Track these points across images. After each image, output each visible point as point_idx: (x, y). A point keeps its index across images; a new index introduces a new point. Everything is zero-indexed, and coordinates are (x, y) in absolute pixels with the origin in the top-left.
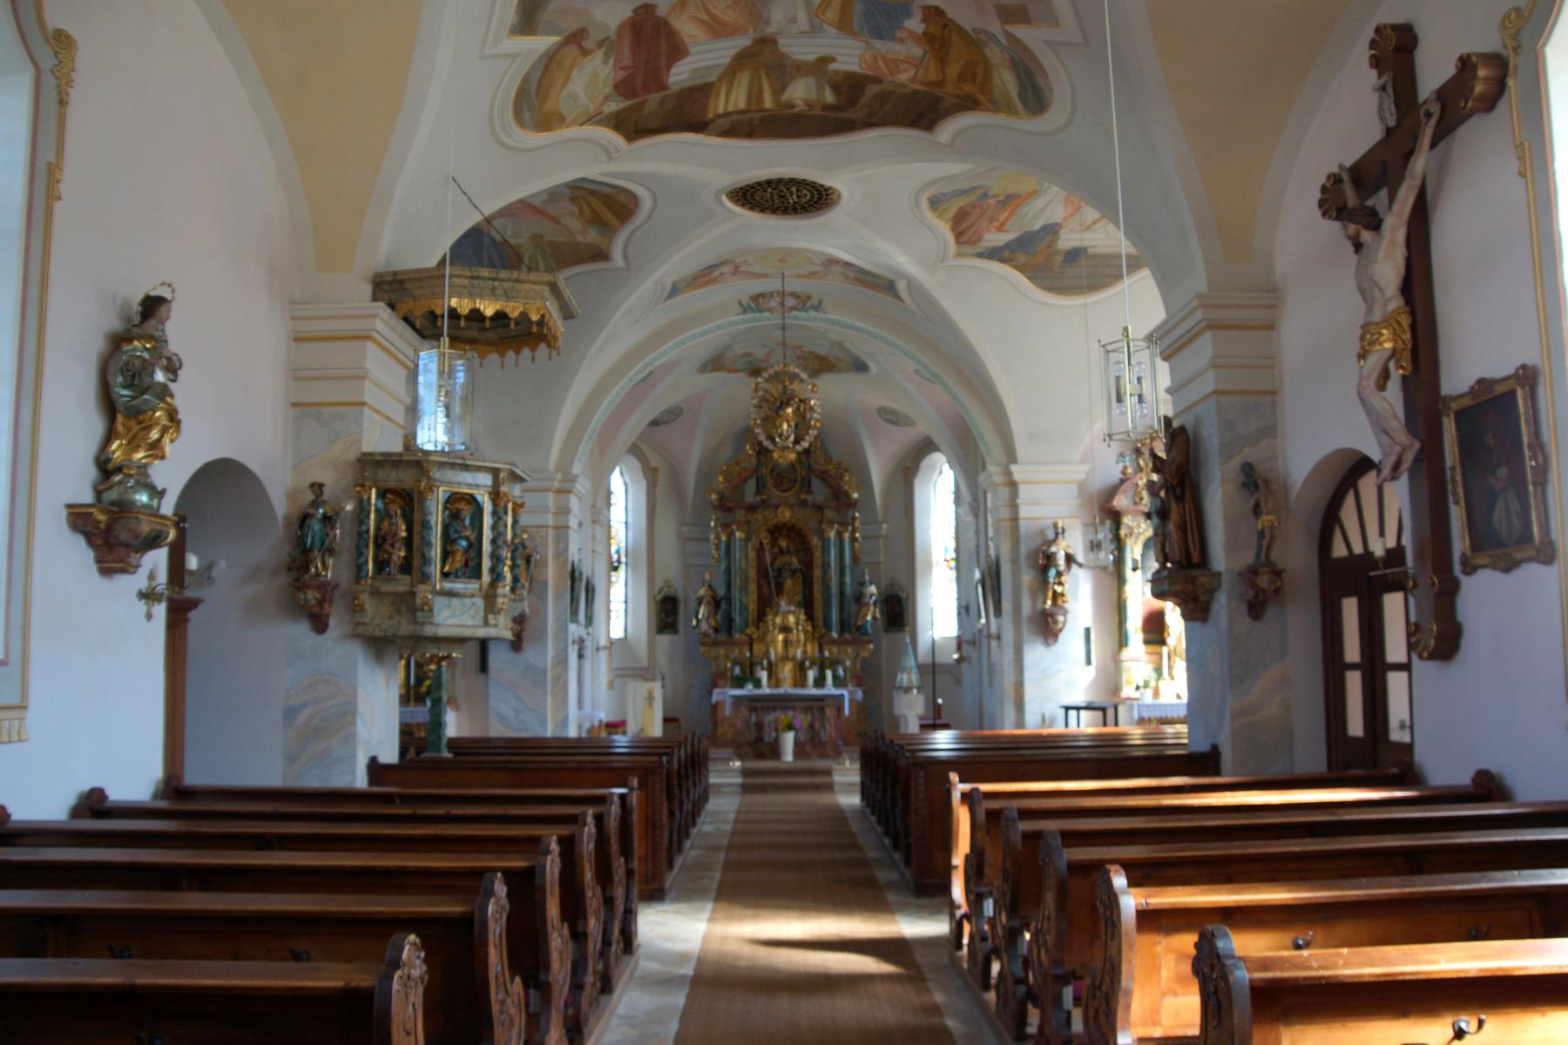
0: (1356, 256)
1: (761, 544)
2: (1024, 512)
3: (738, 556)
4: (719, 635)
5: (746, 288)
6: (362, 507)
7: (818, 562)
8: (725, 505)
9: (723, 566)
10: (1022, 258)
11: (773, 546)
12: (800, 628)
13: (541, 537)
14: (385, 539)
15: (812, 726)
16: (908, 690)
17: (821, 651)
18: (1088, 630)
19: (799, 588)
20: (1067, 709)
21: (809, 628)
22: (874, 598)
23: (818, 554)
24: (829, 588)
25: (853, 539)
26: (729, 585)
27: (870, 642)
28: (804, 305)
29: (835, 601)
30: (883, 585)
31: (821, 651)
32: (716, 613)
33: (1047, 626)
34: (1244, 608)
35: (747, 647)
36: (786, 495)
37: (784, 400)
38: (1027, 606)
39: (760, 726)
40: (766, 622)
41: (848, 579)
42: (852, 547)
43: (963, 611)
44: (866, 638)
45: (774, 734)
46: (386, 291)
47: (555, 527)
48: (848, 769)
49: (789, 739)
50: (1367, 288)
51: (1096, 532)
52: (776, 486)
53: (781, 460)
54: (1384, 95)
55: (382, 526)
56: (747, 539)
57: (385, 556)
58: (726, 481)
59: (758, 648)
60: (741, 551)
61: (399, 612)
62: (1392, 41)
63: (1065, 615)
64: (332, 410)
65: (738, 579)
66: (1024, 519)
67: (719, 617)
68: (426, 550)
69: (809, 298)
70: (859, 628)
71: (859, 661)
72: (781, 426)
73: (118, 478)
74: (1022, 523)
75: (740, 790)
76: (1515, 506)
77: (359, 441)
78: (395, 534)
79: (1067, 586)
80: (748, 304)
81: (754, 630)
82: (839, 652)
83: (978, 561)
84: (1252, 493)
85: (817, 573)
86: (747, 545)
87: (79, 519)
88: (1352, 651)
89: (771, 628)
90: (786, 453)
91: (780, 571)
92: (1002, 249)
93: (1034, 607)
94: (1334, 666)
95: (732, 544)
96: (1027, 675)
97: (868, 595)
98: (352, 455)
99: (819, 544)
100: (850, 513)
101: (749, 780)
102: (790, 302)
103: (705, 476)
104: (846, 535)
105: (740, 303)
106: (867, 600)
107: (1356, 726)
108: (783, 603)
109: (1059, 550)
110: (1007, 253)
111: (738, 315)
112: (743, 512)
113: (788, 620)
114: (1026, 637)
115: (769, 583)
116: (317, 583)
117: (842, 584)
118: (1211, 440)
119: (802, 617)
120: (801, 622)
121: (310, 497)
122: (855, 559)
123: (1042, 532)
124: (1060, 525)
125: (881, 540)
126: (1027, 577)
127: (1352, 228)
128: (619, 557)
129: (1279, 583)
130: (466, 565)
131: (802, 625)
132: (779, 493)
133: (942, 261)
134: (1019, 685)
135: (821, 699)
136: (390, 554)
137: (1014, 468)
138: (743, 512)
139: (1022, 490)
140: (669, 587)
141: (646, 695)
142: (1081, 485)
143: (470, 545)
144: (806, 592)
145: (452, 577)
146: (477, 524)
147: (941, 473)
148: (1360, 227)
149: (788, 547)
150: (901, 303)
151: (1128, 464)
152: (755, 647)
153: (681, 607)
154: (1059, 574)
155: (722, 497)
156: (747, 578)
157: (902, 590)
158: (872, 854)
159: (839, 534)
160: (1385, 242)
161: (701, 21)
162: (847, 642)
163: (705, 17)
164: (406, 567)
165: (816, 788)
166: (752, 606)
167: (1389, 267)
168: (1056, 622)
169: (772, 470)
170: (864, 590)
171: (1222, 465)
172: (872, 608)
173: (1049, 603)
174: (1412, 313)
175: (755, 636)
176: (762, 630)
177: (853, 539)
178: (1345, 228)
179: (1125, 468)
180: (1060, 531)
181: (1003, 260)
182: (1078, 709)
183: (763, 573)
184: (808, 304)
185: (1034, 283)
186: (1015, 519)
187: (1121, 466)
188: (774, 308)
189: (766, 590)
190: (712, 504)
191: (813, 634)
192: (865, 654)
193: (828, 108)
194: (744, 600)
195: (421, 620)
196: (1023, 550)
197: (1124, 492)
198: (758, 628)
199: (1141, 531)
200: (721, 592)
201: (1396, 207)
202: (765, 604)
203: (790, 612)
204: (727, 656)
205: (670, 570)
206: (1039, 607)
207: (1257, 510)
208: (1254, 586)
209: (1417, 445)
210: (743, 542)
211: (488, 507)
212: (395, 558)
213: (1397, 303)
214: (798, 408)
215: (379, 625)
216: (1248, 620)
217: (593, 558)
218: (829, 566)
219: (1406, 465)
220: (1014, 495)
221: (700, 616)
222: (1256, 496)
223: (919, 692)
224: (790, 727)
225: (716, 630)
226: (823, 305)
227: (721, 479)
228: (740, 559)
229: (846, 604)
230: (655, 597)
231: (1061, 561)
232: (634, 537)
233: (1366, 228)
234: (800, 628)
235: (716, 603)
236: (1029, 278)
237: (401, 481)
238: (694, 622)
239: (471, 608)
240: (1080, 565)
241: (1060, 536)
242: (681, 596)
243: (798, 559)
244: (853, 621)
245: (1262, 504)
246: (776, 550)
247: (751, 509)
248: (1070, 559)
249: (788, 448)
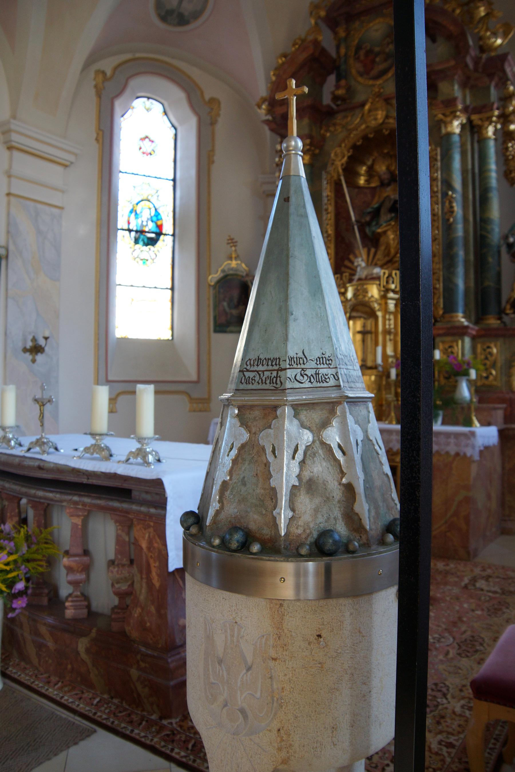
36: (379, 82)
52: (365, 73)
128: (160, 227)
132: (371, 82)
169: (358, 48)
217: (9, 204)
232: (181, 198)
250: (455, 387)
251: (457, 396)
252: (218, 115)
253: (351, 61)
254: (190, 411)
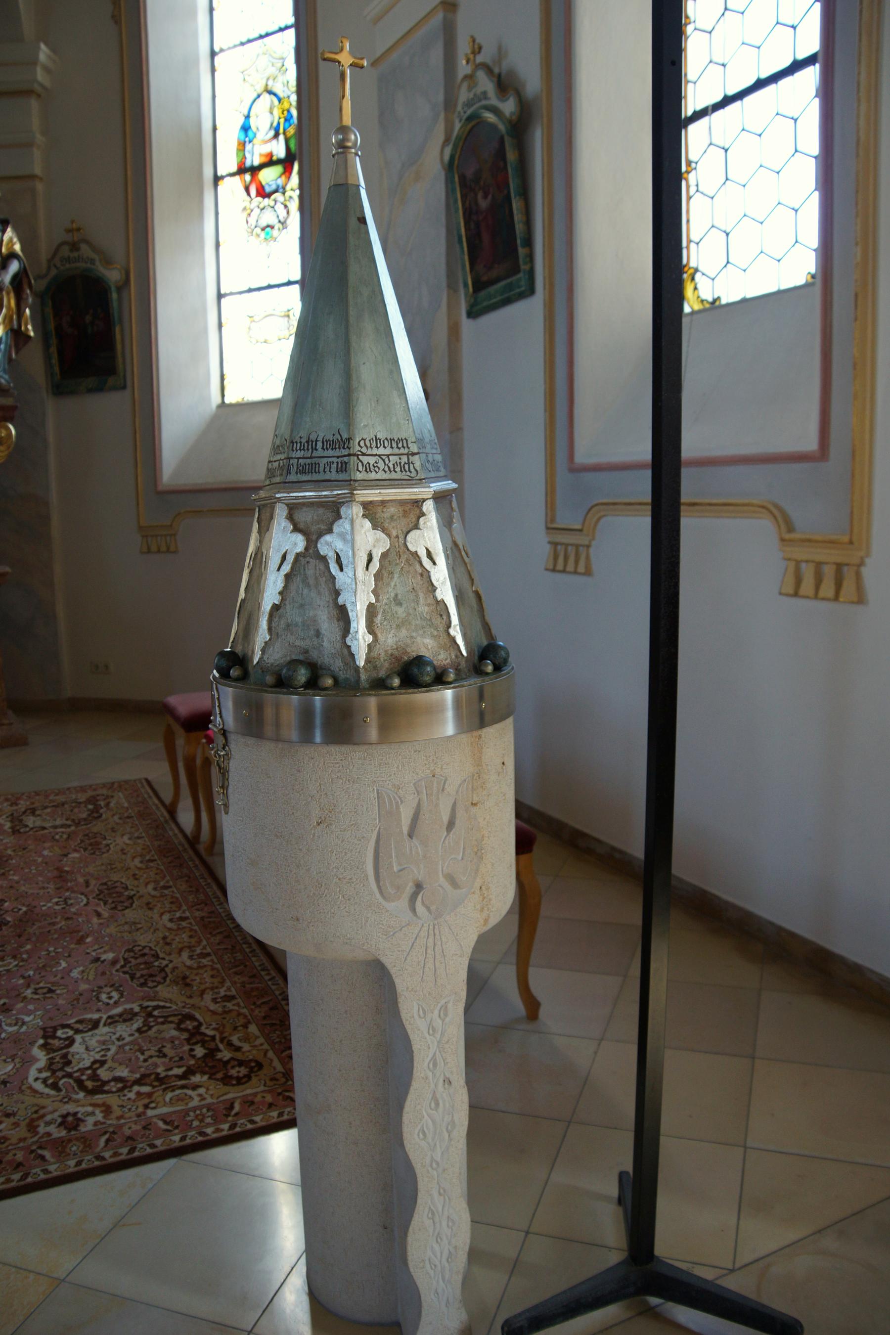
22: (14, 267)
157: (108, 262)
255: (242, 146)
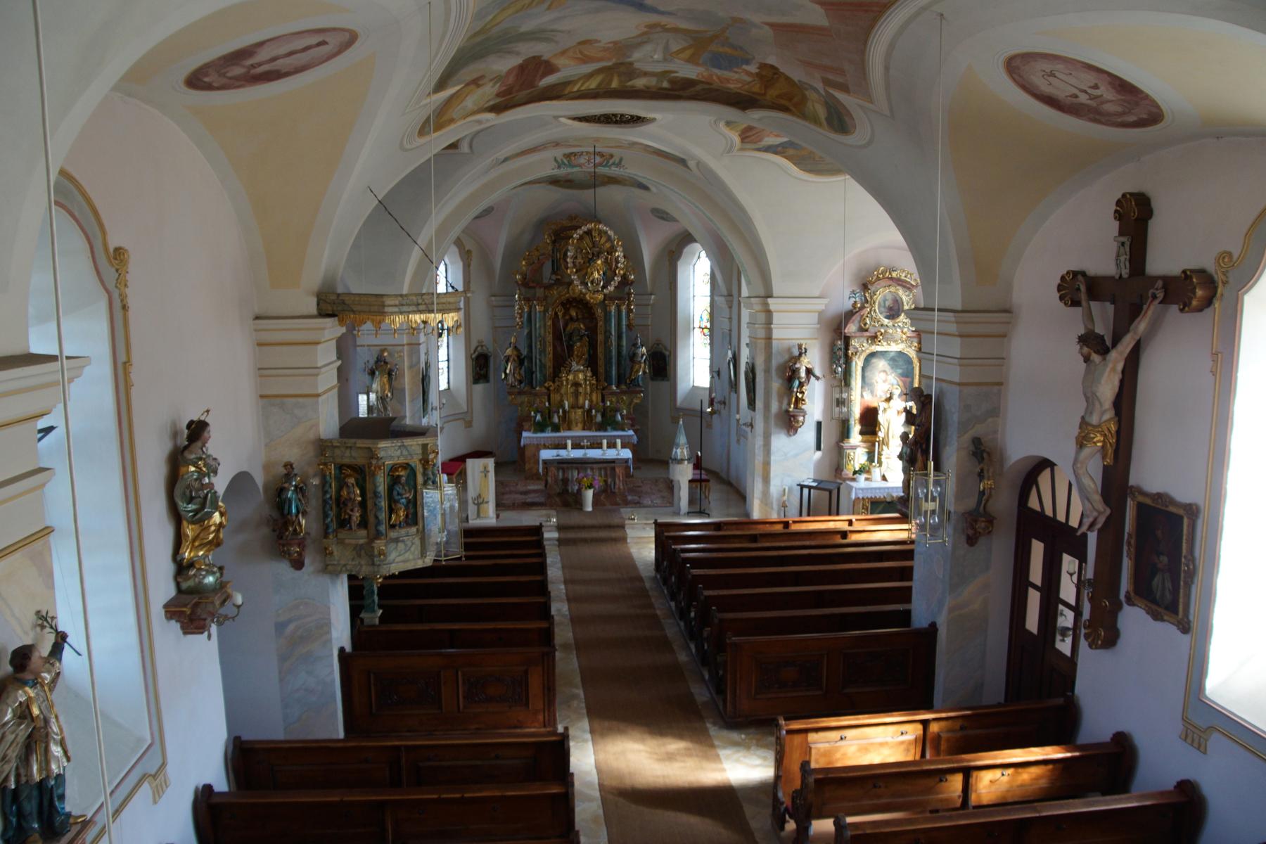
0: (1085, 364)
1: (556, 314)
2: (776, 334)
3: (538, 326)
4: (523, 385)
5: (559, 153)
6: (324, 483)
7: (601, 329)
8: (529, 283)
9: (526, 331)
10: (791, 152)
11: (564, 315)
12: (588, 383)
13: (400, 356)
14: (346, 505)
15: (606, 482)
16: (681, 461)
17: (603, 401)
18: (819, 424)
19: (586, 349)
20: (802, 487)
21: (594, 382)
22: (644, 357)
23: (601, 323)
24: (611, 351)
25: (629, 311)
26: (530, 347)
27: (642, 392)
28: (608, 162)
29: (614, 361)
30: (650, 345)
31: (603, 401)
32: (520, 369)
33: (790, 422)
34: (963, 538)
35: (546, 397)
37: (595, 253)
38: (775, 407)
39: (565, 481)
40: (561, 377)
41: (624, 343)
42: (628, 316)
43: (715, 375)
44: (638, 389)
45: (576, 488)
46: (329, 303)
47: (408, 344)
48: (636, 524)
49: (589, 494)
50: (1091, 398)
51: (841, 392)
53: (592, 301)
54: (1122, 250)
55: (342, 493)
56: (546, 311)
57: (347, 517)
58: (528, 264)
59: (555, 397)
60: (540, 321)
61: (359, 556)
62: (1135, 214)
63: (804, 416)
64: (293, 400)
65: (538, 343)
66: (775, 339)
67: (522, 372)
68: (379, 514)
69: (612, 156)
70: (632, 381)
71: (632, 406)
72: (592, 273)
73: (192, 572)
74: (774, 342)
75: (557, 543)
76: (1169, 585)
77: (317, 425)
78: (354, 500)
79: (806, 393)
80: (562, 160)
81: (551, 383)
82: (618, 402)
83: (730, 344)
84: (980, 463)
85: (600, 338)
86: (545, 314)
87: (172, 610)
88: (1036, 575)
89: (565, 383)
90: (596, 296)
91: (570, 336)
92: (777, 146)
93: (780, 407)
94: (1020, 583)
95: (533, 314)
96: (774, 458)
97: (640, 355)
98: (312, 436)
99: (602, 315)
100: (626, 289)
101: (564, 535)
102: (598, 159)
103: (511, 254)
104: (624, 308)
105: (555, 160)
106: (639, 359)
107: (1032, 623)
108: (574, 364)
109: (801, 365)
110: (780, 149)
111: (553, 169)
112: (542, 290)
113: (578, 378)
114: (773, 429)
115: (563, 345)
116: (296, 541)
117: (619, 346)
118: (954, 415)
119: (589, 374)
120: (588, 378)
121: (283, 471)
122: (629, 326)
123: (789, 350)
124: (804, 346)
125: (650, 307)
126: (776, 385)
127: (1086, 350)
129: (990, 529)
130: (407, 516)
131: (589, 380)
133: (728, 152)
134: (767, 464)
135: (613, 461)
136: (350, 516)
137: (770, 301)
138: (542, 290)
139: (775, 315)
140: (482, 346)
141: (482, 469)
142: (820, 313)
143: (409, 501)
144: (591, 352)
145: (397, 528)
146: (412, 483)
147: (699, 257)
148: (1092, 351)
149: (577, 313)
150: (689, 171)
151: (857, 299)
152: (552, 395)
153: (492, 360)
154: (801, 385)
155: (524, 278)
156: (545, 342)
157: (666, 349)
158: (682, 657)
159: (618, 307)
160: (1108, 369)
161: (577, 58)
162: (623, 393)
163: (580, 56)
164: (364, 524)
165: (615, 540)
166: (549, 364)
167: (1108, 388)
168: (798, 422)
170: (637, 351)
171: (959, 437)
172: (643, 365)
173: (792, 406)
174: (1119, 422)
175: (551, 388)
176: (557, 384)
177: (629, 311)
178: (1081, 348)
179: (855, 302)
180: (803, 351)
181: (776, 153)
182: (810, 488)
183: (557, 336)
184: (611, 162)
185: (798, 167)
186: (769, 338)
187: (853, 300)
188: (584, 164)
189: (559, 349)
190: (517, 282)
191: (597, 388)
192: (636, 401)
193: (665, 89)
194: (543, 361)
195: (378, 563)
196: (774, 363)
197: (853, 322)
198: (554, 382)
199: (864, 349)
200: (525, 352)
201: (1120, 347)
202: (560, 363)
203: (580, 371)
204: (531, 404)
205: (482, 331)
206: (784, 406)
207: (981, 475)
208: (973, 528)
209: (1108, 511)
210: (542, 314)
211: (419, 470)
212: (354, 518)
213: (1110, 414)
214: (607, 258)
215: (345, 565)
216: (966, 546)
218: (611, 334)
219: (1099, 526)
220: (769, 323)
221: (508, 371)
222: (982, 465)
223: (688, 463)
224: (590, 487)
225: (520, 382)
226: (623, 163)
227: (524, 263)
228: (540, 327)
229: (623, 362)
230: (471, 355)
231: (803, 374)
233: (1095, 352)
234: (588, 383)
235: (520, 361)
236: (795, 164)
237: (354, 458)
238: (503, 376)
239: (411, 546)
240: (818, 378)
241: (803, 355)
242: (491, 349)
243: (585, 325)
244: (627, 375)
245: (985, 472)
246: (567, 317)
247: (548, 287)
248: (809, 372)
249: (598, 291)
250: (615, 416)
251: (617, 419)
252: (471, 260)
253: (562, 261)
254: (466, 427)
255: (700, 322)
